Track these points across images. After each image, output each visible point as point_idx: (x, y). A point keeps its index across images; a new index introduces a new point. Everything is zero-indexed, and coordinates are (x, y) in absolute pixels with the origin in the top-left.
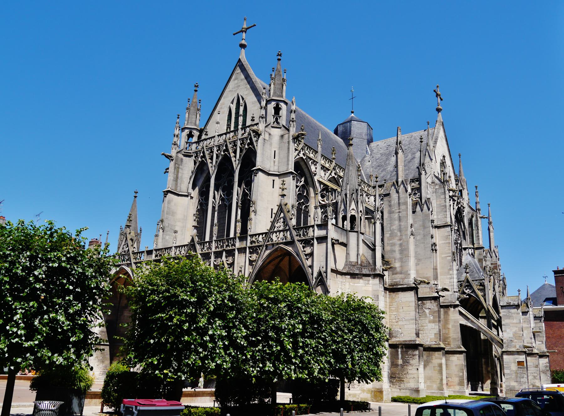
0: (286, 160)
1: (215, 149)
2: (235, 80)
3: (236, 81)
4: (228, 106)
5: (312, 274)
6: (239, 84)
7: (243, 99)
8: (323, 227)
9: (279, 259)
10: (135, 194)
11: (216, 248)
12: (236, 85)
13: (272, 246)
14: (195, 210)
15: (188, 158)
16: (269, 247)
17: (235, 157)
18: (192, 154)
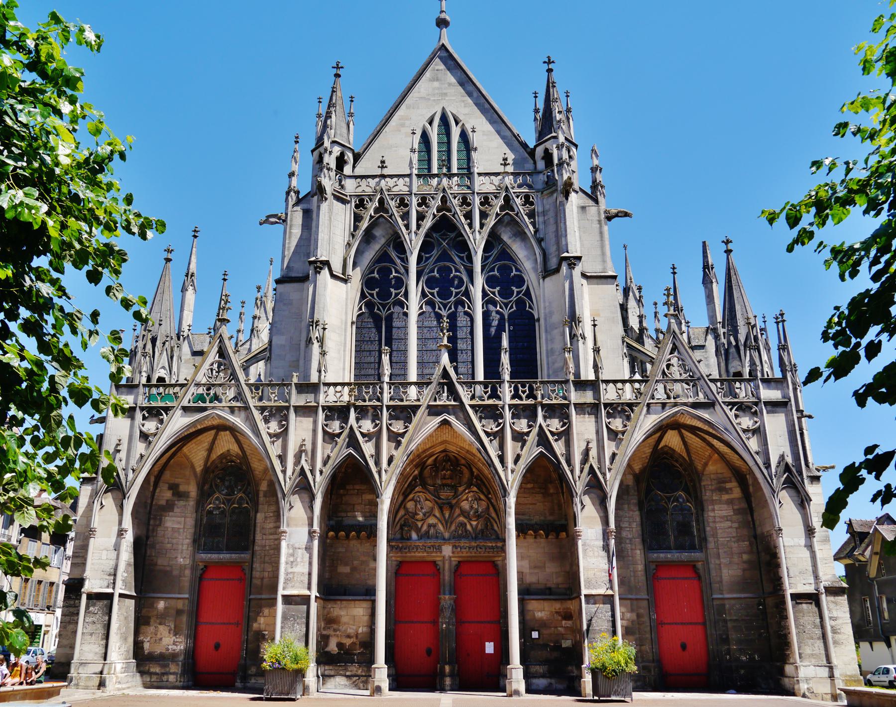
0: (599, 252)
1: (415, 201)
2: (433, 79)
3: (436, 84)
4: (421, 126)
5: (768, 465)
6: (445, 91)
7: (457, 123)
8: (773, 383)
9: (658, 435)
10: (165, 255)
11: (513, 397)
12: (437, 91)
13: (660, 408)
14: (356, 314)
15: (340, 204)
16: (652, 407)
17: (471, 225)
18: (348, 198)
